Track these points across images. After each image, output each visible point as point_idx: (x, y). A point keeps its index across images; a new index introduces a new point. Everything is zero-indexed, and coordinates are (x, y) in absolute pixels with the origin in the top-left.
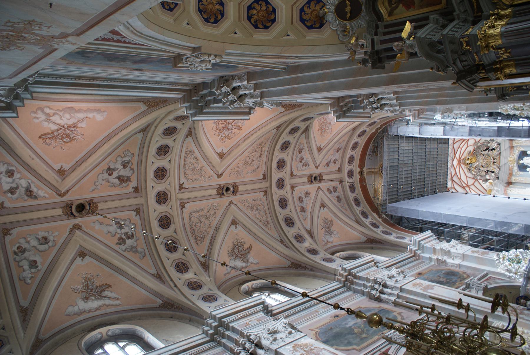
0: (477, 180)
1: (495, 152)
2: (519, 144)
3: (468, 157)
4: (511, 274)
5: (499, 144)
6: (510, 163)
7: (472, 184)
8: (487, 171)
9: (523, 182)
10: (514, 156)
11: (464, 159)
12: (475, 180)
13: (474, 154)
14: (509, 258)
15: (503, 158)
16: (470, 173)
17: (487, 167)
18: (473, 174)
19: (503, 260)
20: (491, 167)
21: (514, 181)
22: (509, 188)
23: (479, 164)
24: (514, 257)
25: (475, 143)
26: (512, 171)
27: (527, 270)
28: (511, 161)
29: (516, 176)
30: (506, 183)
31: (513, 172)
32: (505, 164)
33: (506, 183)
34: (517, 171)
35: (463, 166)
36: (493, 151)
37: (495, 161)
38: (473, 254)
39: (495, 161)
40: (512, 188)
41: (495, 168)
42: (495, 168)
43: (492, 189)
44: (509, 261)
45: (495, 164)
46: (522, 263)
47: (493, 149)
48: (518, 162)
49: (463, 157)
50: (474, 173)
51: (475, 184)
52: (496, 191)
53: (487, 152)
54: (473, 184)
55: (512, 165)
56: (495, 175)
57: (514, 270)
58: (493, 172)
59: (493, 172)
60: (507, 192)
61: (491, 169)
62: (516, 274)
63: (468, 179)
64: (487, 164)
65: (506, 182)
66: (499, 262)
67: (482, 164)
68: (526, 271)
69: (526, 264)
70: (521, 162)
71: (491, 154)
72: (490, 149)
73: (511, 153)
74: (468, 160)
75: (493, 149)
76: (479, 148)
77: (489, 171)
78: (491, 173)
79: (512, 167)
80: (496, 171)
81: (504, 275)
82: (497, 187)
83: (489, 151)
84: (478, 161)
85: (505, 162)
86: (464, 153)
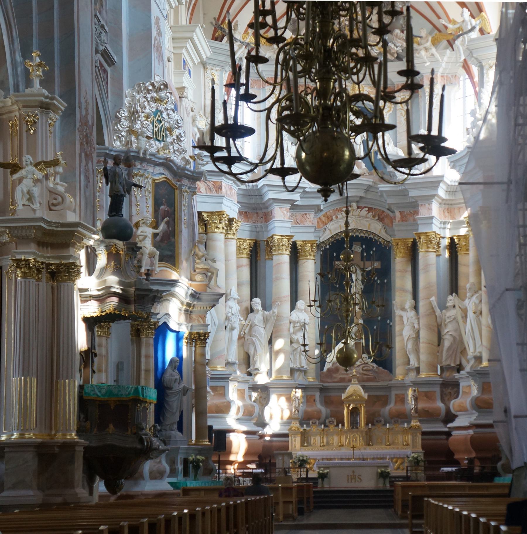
4: (126, 123)
14: (162, 113)
19: (155, 100)
24: (167, 125)
27: (148, 157)
38: (153, 21)
44: (155, 114)
46: (157, 143)
57: (138, 126)
62: (131, 131)
66: (149, 91)
68: (145, 153)
69: (158, 152)
81: (119, 105)
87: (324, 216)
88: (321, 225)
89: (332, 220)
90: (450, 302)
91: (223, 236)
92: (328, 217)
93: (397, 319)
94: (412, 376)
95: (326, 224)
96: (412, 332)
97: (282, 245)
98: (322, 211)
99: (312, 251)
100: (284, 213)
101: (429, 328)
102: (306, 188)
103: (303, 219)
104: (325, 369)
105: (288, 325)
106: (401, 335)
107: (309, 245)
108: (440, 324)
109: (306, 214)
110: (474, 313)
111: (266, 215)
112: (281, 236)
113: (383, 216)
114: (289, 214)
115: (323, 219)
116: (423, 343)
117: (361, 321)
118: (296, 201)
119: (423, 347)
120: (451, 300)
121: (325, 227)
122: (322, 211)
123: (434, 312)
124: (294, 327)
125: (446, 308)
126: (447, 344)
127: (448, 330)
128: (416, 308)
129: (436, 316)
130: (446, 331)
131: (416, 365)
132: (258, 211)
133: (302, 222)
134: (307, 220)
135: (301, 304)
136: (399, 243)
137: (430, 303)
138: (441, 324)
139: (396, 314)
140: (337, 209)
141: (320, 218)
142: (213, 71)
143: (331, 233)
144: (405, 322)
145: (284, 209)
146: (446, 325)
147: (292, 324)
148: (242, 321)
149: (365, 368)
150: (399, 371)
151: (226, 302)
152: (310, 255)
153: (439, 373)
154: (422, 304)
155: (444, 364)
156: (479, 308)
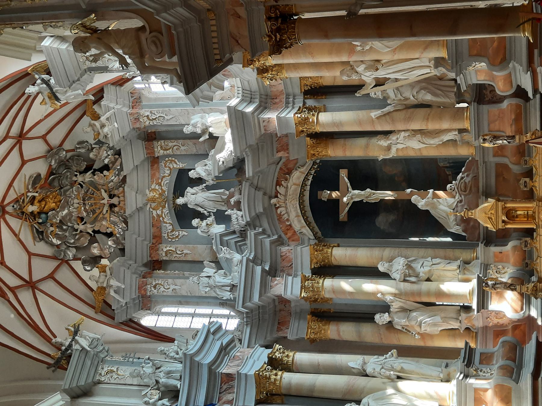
0: (67, 262)
1: (111, 177)
2: (169, 152)
3: (30, 194)
5: (118, 153)
6: (153, 205)
7: (46, 274)
8: (94, 231)
9: (189, 258)
10: (160, 184)
11: (16, 201)
12: (55, 263)
13: (50, 184)
15: (134, 193)
16: (42, 243)
17: (95, 220)
18: (52, 245)
20: (104, 218)
21: (165, 258)
22: (149, 280)
23: (70, 214)
25: (49, 152)
26: (160, 229)
28: (153, 200)
29: (171, 243)
30: (145, 265)
31: (163, 230)
32: (139, 210)
33: (145, 265)
34: (171, 227)
35: (15, 223)
36: (105, 172)
37: (115, 201)
39: (115, 201)
40: (159, 278)
41: (115, 224)
42: (115, 224)
43: (105, 285)
45: (116, 209)
47: (106, 168)
48: (174, 203)
49: (11, 196)
50: (55, 241)
51: (58, 276)
52: (115, 292)
53: (88, 177)
54: (51, 276)
55: (159, 212)
56: (116, 242)
58: (110, 235)
59: (110, 235)
60: (146, 290)
61: (104, 225)
63: (35, 261)
64: (94, 212)
65: (145, 261)
67: (79, 212)
70: (180, 201)
71: (102, 182)
72: (96, 167)
73: (153, 176)
74: (32, 204)
75: (106, 168)
76: (64, 164)
77: (98, 232)
78: (104, 237)
79: (158, 215)
80: (118, 230)
82: (119, 281)
83: (94, 174)
84: (67, 204)
85: (140, 205)
86: (15, 184)
87: (287, 234)
88: (296, 237)
89: (290, 225)
90: (377, 94)
91: (287, 376)
92: (288, 230)
93: (401, 154)
94: (469, 137)
95: (295, 232)
96: (415, 138)
97: (313, 287)
98: (280, 237)
99: (322, 250)
100: (277, 284)
101: (409, 119)
102: (248, 260)
103: (288, 259)
104: (464, 234)
105: (406, 284)
106: (420, 149)
107: (316, 253)
108: (404, 107)
109: (281, 256)
110: (377, 69)
111: (282, 301)
112: (302, 288)
113: (285, 169)
114: (278, 278)
115: (289, 234)
116: (427, 125)
117: (409, 190)
118: (263, 270)
119: (431, 126)
120: (375, 94)
121: (298, 233)
122: (280, 237)
123: (389, 113)
124: (410, 276)
125: (385, 99)
126: (428, 97)
127: (411, 96)
128: (387, 133)
129: (394, 111)
130: (412, 98)
131: (457, 133)
132: (277, 309)
133: (290, 261)
134: (288, 255)
135: (382, 268)
136: (312, 152)
137: (378, 118)
138: (405, 104)
139: (395, 155)
140: (278, 220)
141: (289, 239)
142: (103, 373)
143: (305, 227)
144: (404, 146)
145: (272, 284)
146: (406, 99)
147: (408, 279)
148: (392, 354)
149: (463, 189)
150: (463, 152)
151: (367, 375)
152: (327, 253)
153: (465, 105)
154: (379, 128)
155: (453, 100)
156: (372, 63)
